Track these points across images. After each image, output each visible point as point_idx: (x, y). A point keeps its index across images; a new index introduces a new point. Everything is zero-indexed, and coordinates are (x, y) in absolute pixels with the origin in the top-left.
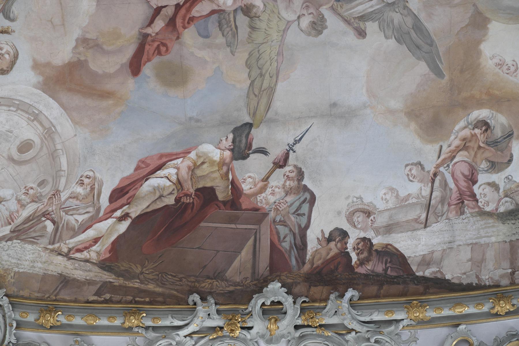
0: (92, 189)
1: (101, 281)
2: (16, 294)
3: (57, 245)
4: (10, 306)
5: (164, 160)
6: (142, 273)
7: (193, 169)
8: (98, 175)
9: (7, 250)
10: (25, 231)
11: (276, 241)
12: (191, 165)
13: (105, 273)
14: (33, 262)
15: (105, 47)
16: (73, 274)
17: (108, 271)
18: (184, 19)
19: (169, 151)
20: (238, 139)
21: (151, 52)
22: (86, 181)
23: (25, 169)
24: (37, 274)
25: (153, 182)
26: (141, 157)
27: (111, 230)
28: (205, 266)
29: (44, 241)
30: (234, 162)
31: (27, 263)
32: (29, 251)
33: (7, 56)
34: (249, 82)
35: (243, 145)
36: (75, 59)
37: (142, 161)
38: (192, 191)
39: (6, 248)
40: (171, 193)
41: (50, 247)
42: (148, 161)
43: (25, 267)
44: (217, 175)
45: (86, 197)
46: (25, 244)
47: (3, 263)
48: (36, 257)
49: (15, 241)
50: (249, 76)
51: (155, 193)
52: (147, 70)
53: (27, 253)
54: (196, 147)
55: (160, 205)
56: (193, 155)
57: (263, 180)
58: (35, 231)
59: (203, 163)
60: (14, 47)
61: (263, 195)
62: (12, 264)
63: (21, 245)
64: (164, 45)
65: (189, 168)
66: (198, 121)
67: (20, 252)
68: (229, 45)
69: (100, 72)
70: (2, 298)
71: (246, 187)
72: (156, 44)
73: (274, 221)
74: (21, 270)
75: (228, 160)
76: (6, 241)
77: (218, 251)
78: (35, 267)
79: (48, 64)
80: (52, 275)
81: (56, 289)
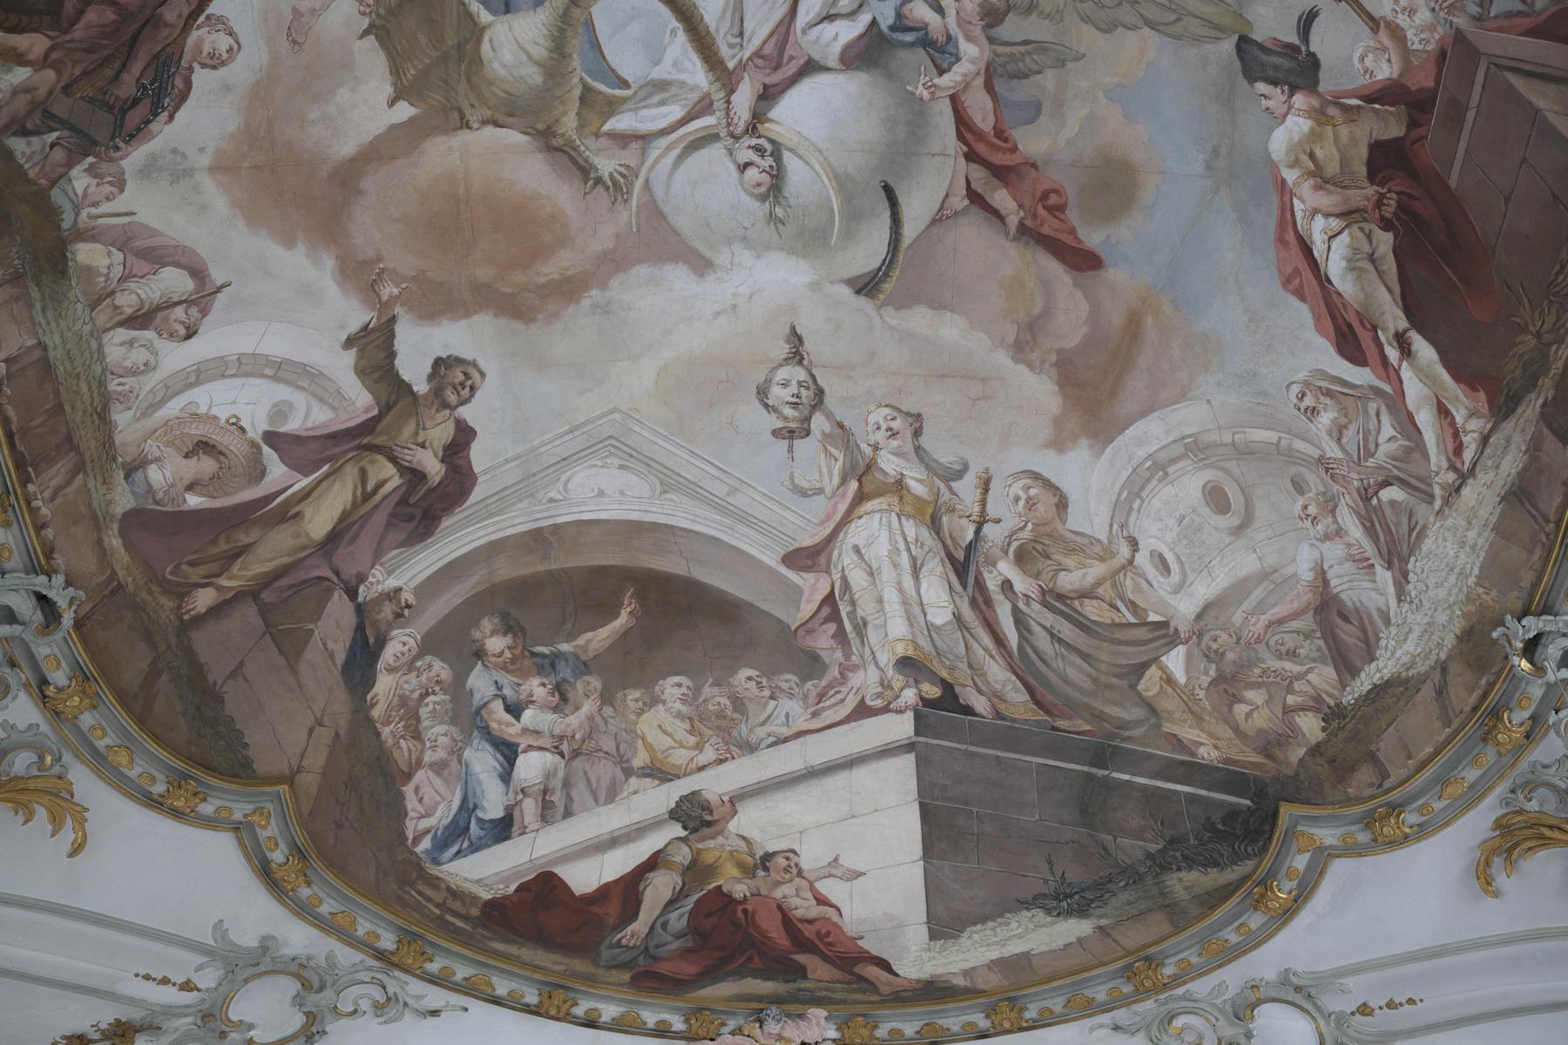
0: (1328, 393)
1: (1537, 423)
2: (1525, 596)
3: (1437, 491)
4: (1544, 617)
5: (1291, 236)
6: (1538, 335)
7: (1320, 178)
8: (1301, 376)
9: (1427, 587)
10: (1393, 541)
11: (1527, 22)
12: (1311, 181)
13: (1520, 410)
14: (1462, 544)
15: (1036, 311)
16: (1509, 475)
17: (1518, 404)
18: (998, 148)
19: (1272, 223)
20: (1270, 73)
21: (1055, 223)
22: (1309, 401)
23: (1262, 511)
24: (1492, 545)
25: (1336, 268)
26: (1276, 283)
27: (1424, 375)
28: (1553, 195)
29: (1422, 510)
30: (1321, 88)
31: (1462, 556)
32: (1438, 547)
33: (1033, 492)
34: (1146, 31)
35: (1286, 63)
36: (1054, 372)
37: (1286, 283)
38: (1371, 191)
39: (1421, 587)
40: (1369, 237)
41: (1438, 504)
42: (1289, 270)
43: (1471, 563)
44: (1344, 131)
45: (1343, 410)
46: (1421, 550)
47: (1451, 599)
48: (1454, 536)
49: (1410, 566)
50: (1134, 28)
51: (1361, 270)
52: (1092, 237)
53: (1441, 550)
54: (1274, 167)
55: (1390, 265)
56: (1290, 176)
57: (1375, 31)
58: (1397, 525)
59: (1312, 156)
60: (1017, 475)
61: (1410, 34)
62: (1459, 584)
63: (1422, 558)
64: (1045, 196)
65: (1317, 188)
66: (1216, 153)
67: (1436, 564)
68: (1061, 63)
69: (1085, 330)
70: (1524, 627)
71: (1385, 70)
72: (1042, 212)
73: (1478, 19)
74: (1476, 571)
75: (1315, 102)
76: (1408, 582)
77: (1524, 160)
78: (1475, 545)
79: (1058, 423)
80: (1501, 515)
81: (1533, 517)
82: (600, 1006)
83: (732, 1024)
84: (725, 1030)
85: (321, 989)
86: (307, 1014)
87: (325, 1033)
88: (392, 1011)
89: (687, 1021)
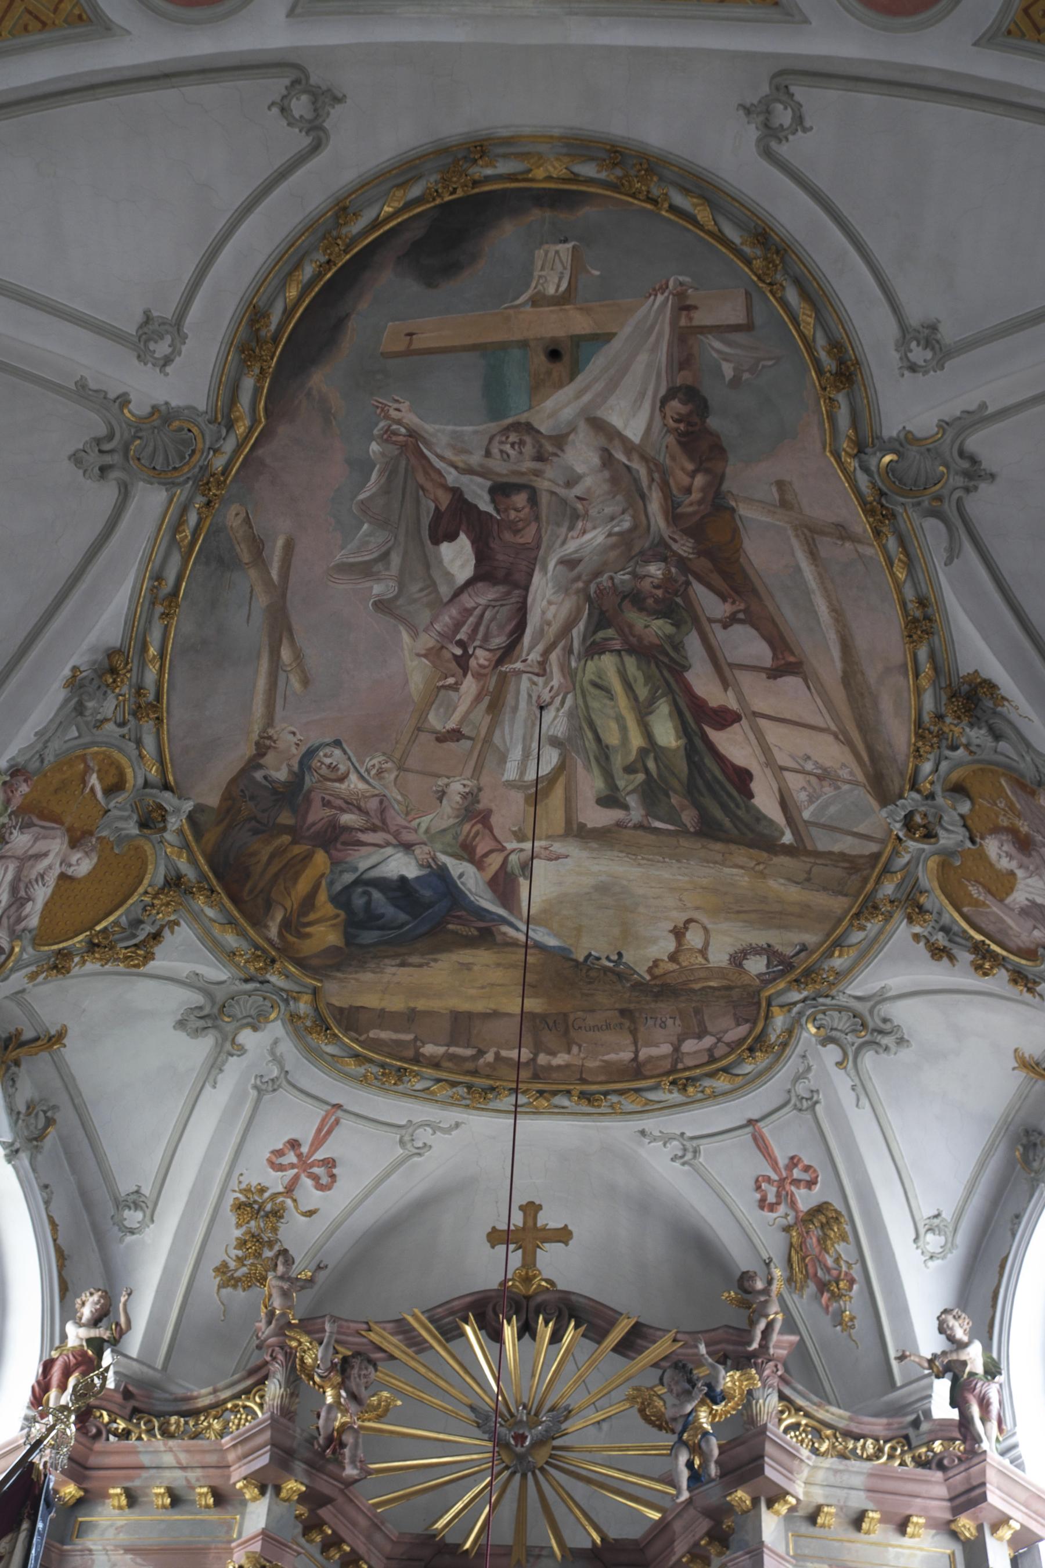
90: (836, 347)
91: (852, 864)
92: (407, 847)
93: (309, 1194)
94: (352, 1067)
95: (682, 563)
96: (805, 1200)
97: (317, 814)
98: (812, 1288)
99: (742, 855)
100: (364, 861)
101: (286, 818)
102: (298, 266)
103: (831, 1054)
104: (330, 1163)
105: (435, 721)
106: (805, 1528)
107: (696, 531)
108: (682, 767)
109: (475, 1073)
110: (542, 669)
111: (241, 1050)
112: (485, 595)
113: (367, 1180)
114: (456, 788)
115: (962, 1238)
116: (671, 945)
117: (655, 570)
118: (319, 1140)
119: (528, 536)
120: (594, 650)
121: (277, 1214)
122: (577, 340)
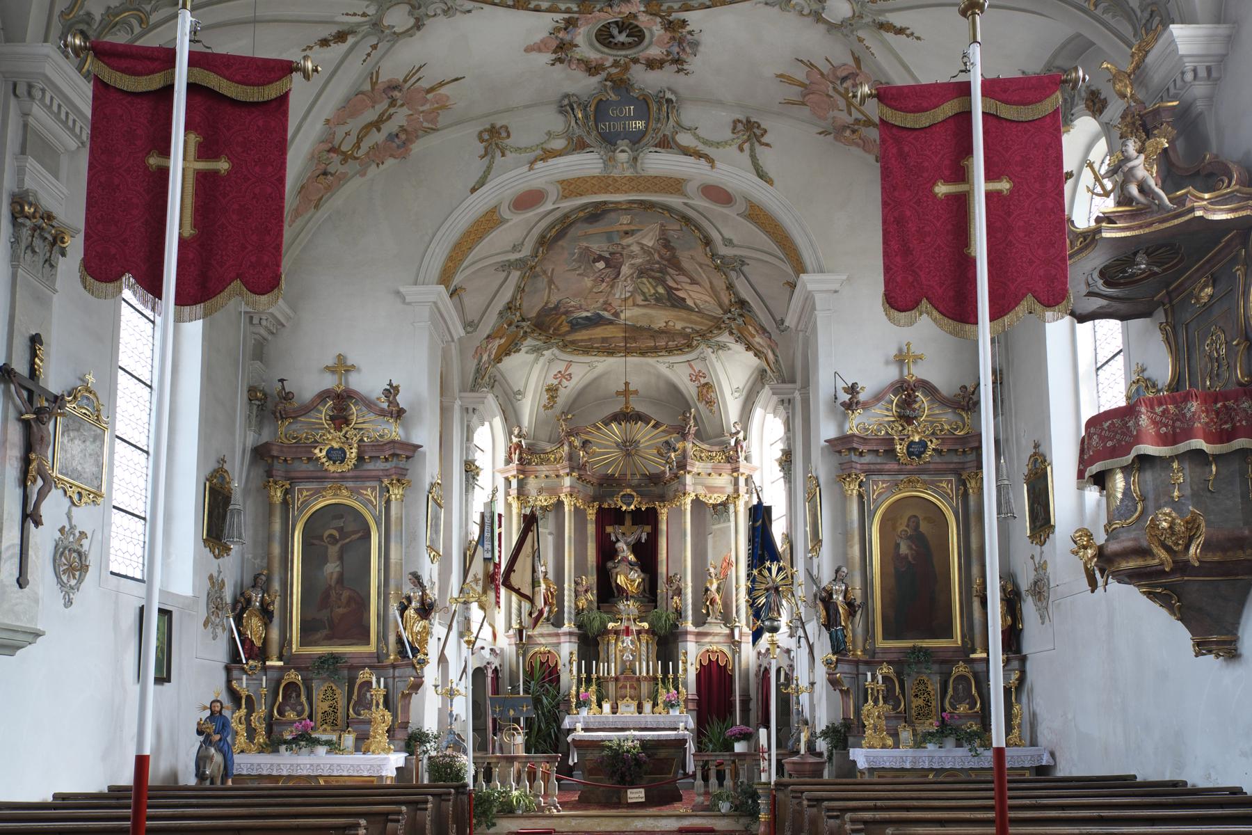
82: (540, 3)
83: (598, 7)
84: (596, 9)
85: (419, 8)
86: (416, 18)
87: (424, 25)
88: (451, 12)
89: (579, 7)
90: (705, 237)
91: (715, 318)
92: (588, 311)
93: (565, 383)
94: (576, 352)
95: (665, 265)
96: (703, 381)
97: (562, 310)
98: (704, 402)
99: (683, 311)
100: (575, 315)
101: (554, 312)
102: (554, 227)
103: (710, 350)
104: (570, 375)
105: (594, 290)
106: (697, 476)
107: (668, 260)
108: (667, 297)
109: (609, 349)
110: (625, 280)
111: (542, 355)
112: (608, 270)
113: (581, 376)
114: (601, 300)
115: (744, 393)
116: (665, 324)
117: (657, 266)
118: (566, 370)
119: (621, 260)
120: (639, 277)
121: (557, 390)
122: (633, 230)
